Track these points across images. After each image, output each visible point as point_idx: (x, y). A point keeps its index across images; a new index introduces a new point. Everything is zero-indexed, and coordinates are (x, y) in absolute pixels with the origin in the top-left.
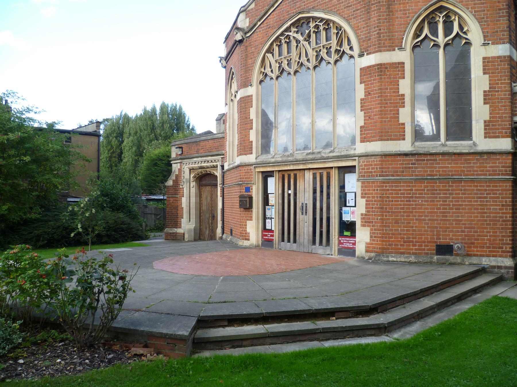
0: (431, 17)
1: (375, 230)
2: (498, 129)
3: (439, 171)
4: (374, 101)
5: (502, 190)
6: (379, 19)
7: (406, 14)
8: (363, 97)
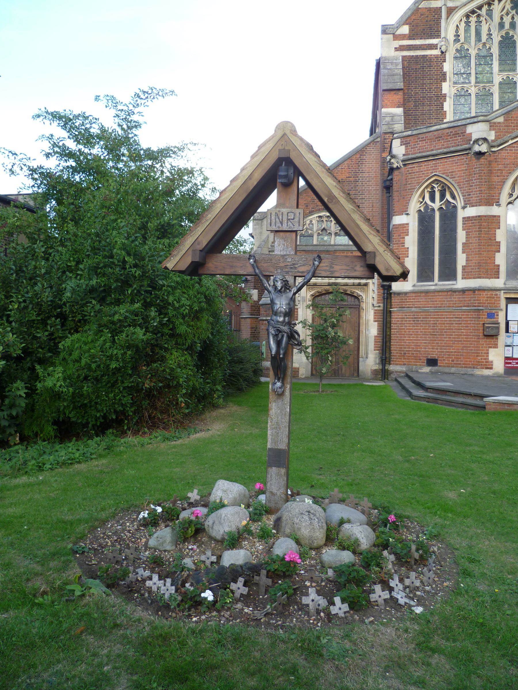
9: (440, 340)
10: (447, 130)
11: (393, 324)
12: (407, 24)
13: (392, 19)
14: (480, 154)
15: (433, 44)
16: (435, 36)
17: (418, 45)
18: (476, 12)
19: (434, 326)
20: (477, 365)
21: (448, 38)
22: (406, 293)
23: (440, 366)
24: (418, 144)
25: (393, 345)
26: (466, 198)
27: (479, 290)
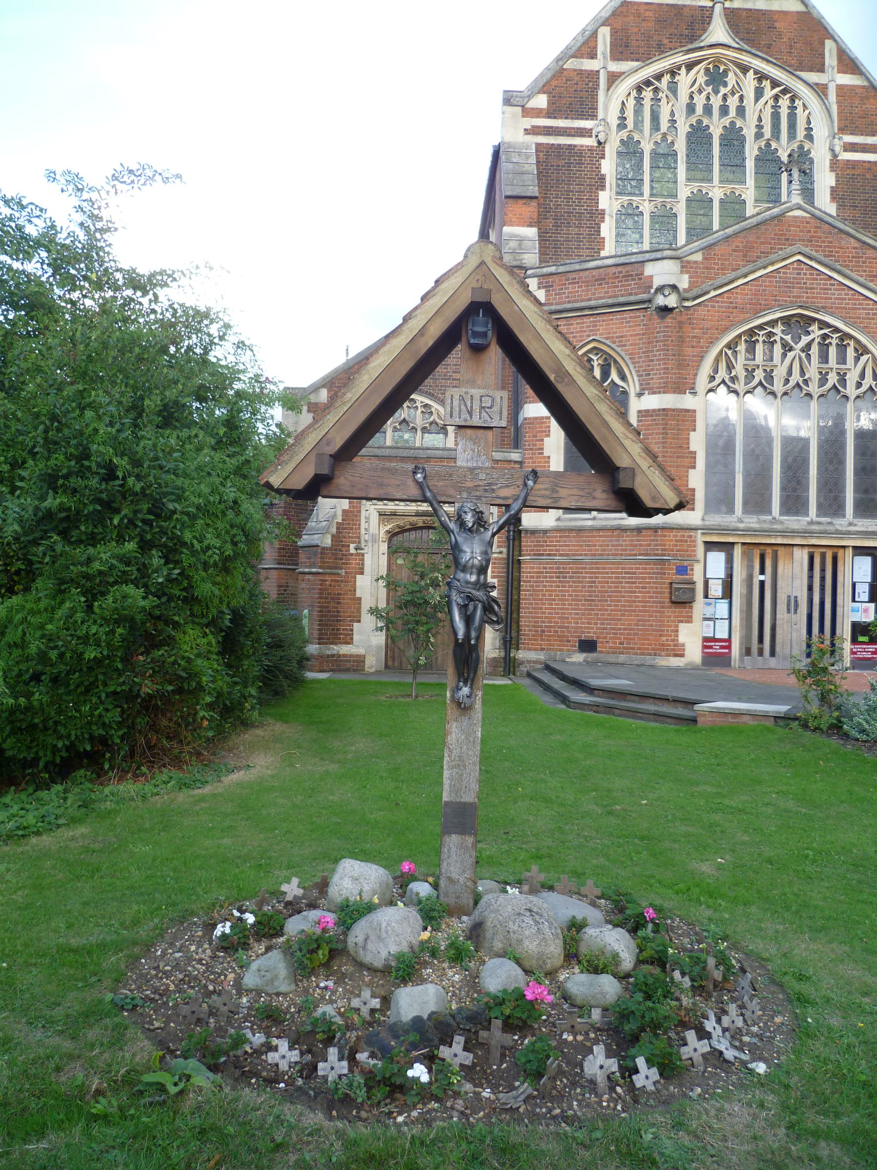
9: (600, 610)
10: (614, 268)
11: (524, 582)
12: (544, 93)
13: (521, 83)
14: (665, 310)
15: (585, 129)
17: (560, 128)
18: (652, 84)
19: (592, 587)
20: (660, 650)
21: (609, 121)
22: (545, 532)
23: (601, 652)
24: (566, 289)
25: (523, 617)
26: (643, 380)
27: (663, 528)
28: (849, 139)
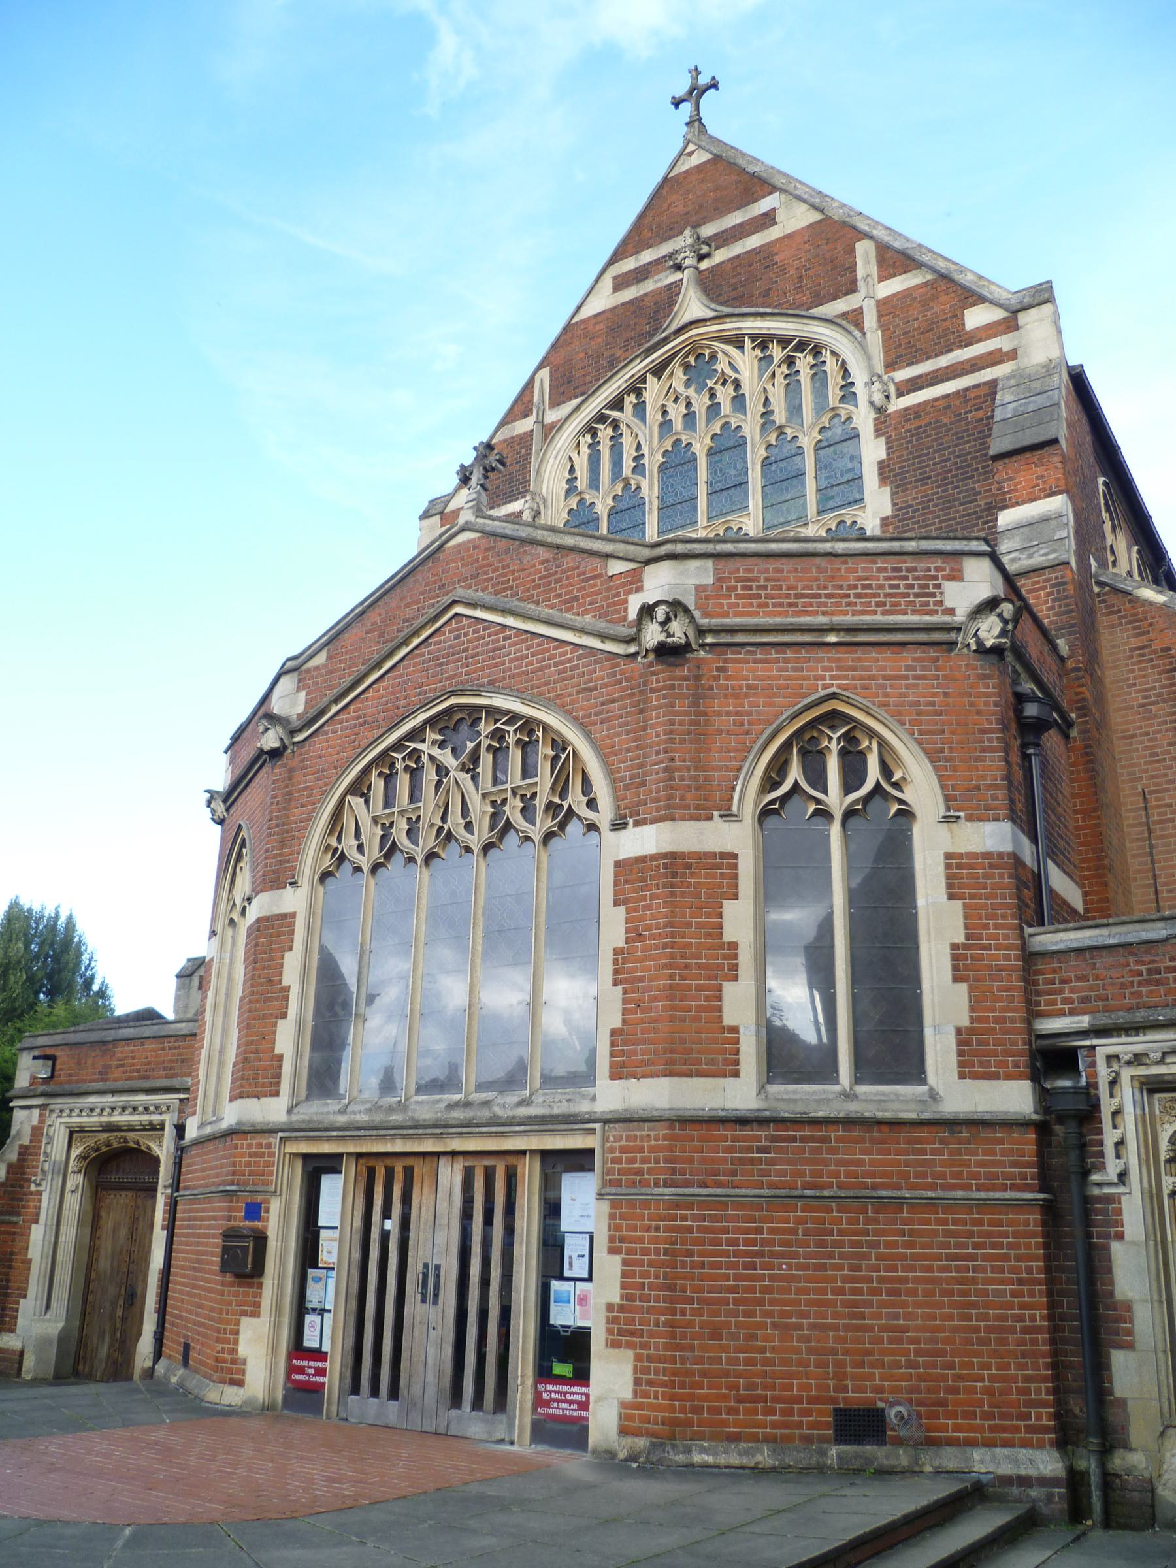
0: (807, 736)
1: (650, 1359)
2: (994, 1053)
3: (837, 1174)
4: (651, 958)
5: (1016, 1235)
6: (671, 732)
7: (742, 724)
8: (621, 944)
16: (519, 493)
28: (904, 374)
